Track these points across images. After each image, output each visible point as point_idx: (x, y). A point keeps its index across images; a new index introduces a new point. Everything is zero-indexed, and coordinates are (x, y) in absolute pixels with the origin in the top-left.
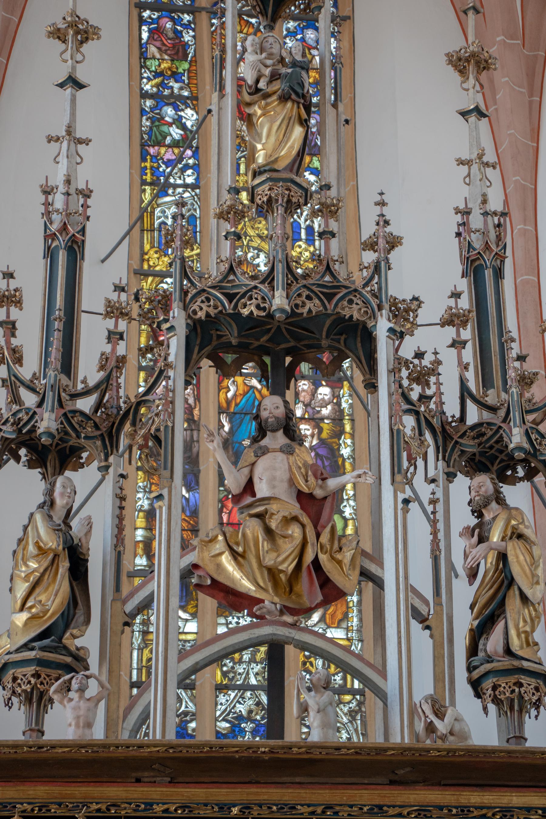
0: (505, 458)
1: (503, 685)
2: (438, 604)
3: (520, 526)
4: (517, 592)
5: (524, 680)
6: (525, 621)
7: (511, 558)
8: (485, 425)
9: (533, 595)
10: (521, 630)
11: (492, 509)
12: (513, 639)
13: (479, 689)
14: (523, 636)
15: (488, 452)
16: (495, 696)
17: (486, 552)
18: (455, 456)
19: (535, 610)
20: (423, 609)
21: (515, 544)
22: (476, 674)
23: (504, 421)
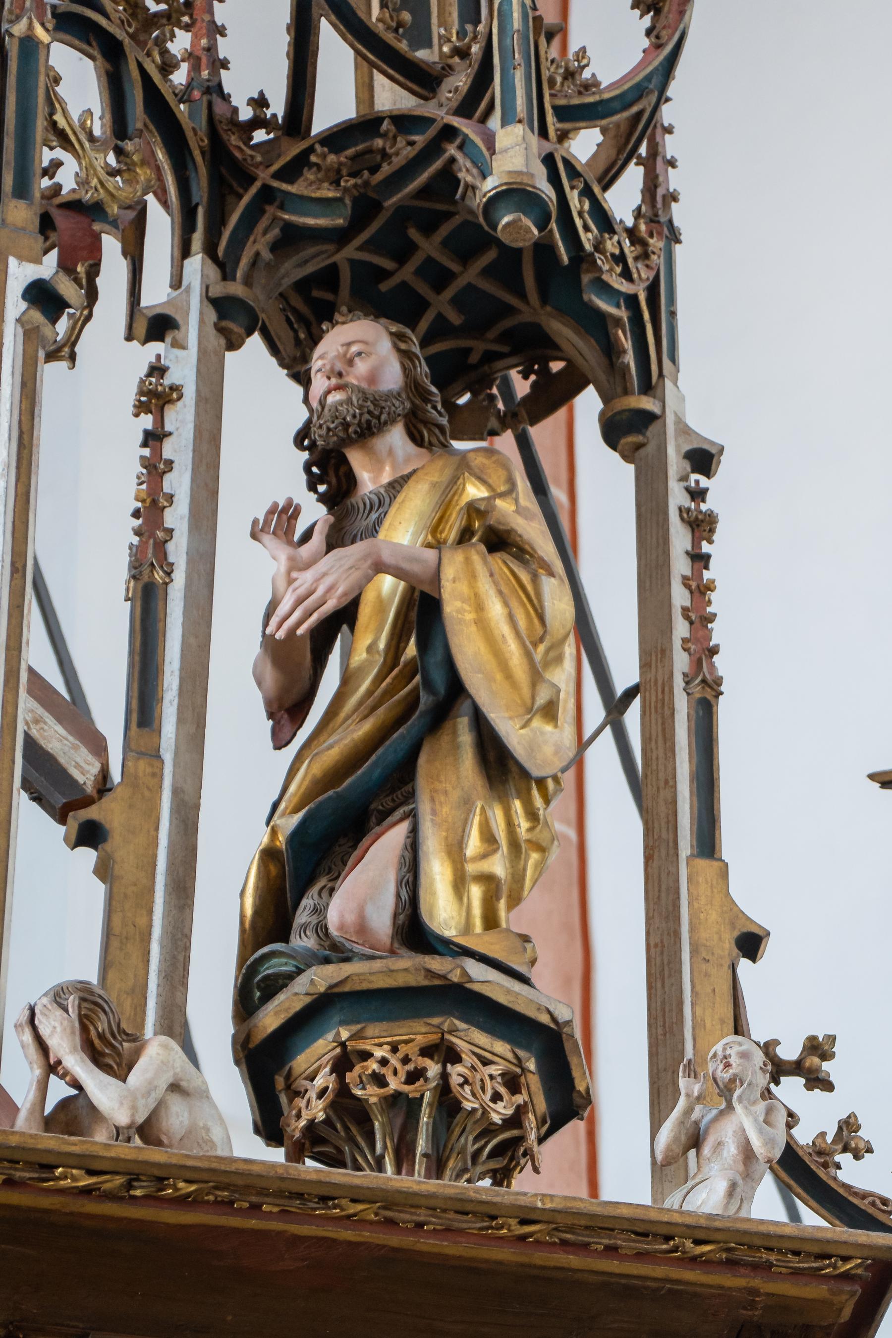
0: (455, 318)
1: (379, 1053)
2: (141, 754)
3: (498, 502)
4: (466, 738)
5: (470, 1038)
6: (489, 838)
7: (453, 606)
8: (386, 125)
9: (532, 748)
10: (471, 868)
11: (391, 452)
12: (434, 894)
13: (280, 1082)
14: (476, 892)
15: (385, 274)
16: (343, 1090)
17: (356, 575)
18: (259, 244)
19: (532, 815)
20: (82, 768)
21: (476, 558)
22: (270, 1018)
23: (466, 108)
